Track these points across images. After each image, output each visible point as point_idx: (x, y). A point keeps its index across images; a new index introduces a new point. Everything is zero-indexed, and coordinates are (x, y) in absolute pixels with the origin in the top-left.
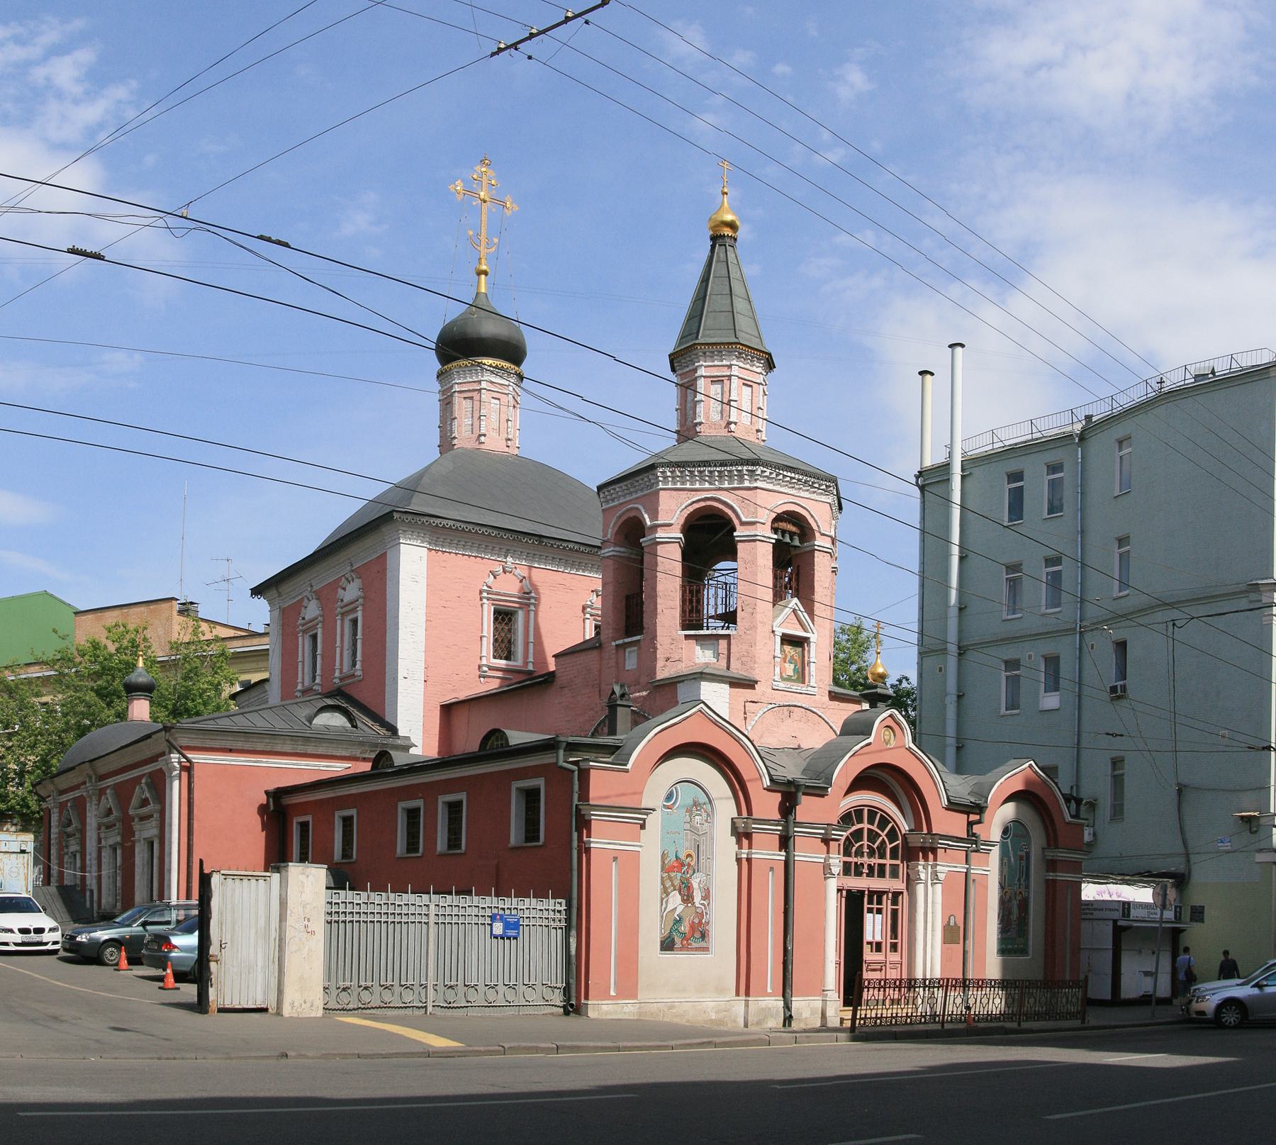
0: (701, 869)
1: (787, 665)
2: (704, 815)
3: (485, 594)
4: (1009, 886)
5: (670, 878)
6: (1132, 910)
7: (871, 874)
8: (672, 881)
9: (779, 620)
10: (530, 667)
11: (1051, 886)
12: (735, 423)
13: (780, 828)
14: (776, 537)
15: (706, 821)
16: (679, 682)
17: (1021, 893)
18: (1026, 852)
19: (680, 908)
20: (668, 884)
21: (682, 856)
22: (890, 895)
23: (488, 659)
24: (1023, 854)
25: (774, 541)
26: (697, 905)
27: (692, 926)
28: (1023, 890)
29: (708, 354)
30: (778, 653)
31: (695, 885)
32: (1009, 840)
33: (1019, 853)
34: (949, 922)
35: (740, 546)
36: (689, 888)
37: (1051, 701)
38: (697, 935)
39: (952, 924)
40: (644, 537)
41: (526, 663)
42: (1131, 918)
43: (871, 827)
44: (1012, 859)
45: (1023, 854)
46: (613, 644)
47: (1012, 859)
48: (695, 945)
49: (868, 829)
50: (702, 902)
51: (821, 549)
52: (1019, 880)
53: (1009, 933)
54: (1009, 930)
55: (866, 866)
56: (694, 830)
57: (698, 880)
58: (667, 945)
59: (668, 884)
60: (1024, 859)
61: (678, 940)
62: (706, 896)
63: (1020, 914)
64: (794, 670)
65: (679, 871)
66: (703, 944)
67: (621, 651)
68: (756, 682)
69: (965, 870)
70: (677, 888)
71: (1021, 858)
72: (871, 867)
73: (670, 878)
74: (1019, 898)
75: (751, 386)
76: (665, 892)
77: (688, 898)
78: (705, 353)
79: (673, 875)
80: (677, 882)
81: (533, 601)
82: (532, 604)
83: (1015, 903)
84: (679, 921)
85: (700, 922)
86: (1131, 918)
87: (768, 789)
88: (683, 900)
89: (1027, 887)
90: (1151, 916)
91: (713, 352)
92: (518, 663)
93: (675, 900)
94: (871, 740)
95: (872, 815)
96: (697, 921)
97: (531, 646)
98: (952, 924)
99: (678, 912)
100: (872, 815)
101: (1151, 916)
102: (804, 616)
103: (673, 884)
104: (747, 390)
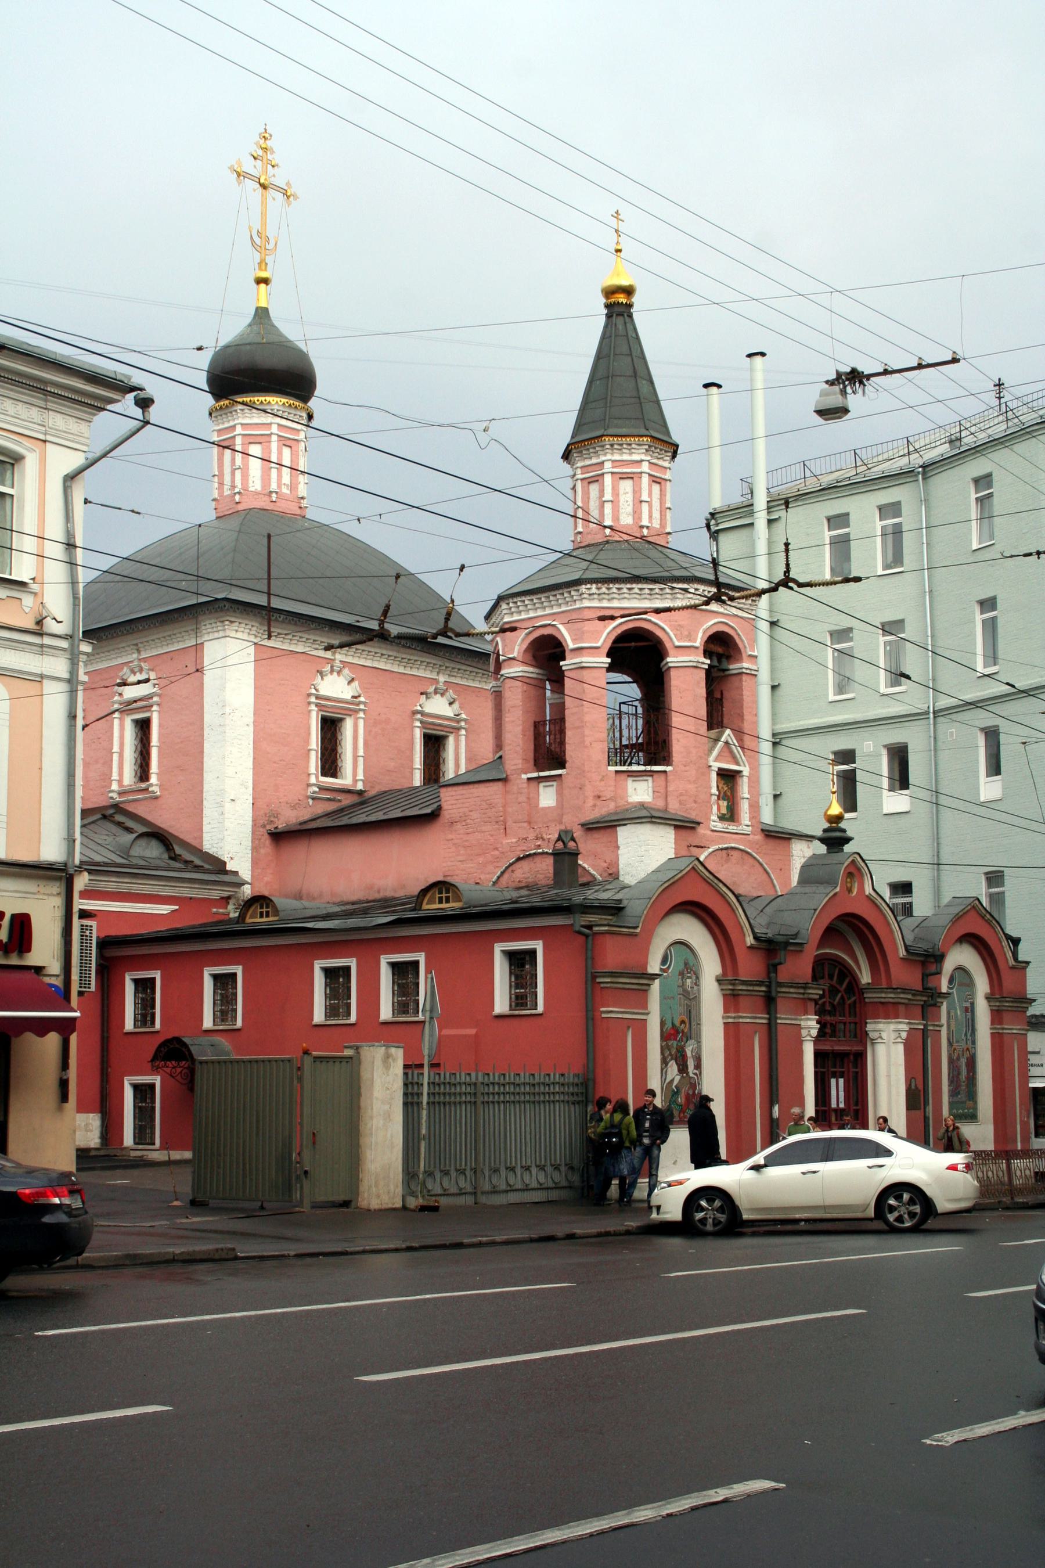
0: (693, 1036)
1: (721, 802)
2: (694, 977)
3: (313, 699)
8: (669, 1050)
9: (715, 753)
10: (360, 786)
13: (763, 989)
14: (708, 661)
15: (696, 984)
16: (620, 825)
17: (968, 1049)
19: (677, 1079)
20: (667, 1053)
21: (677, 1024)
22: (852, 1057)
23: (317, 778)
24: (968, 1005)
25: (707, 667)
26: (691, 1075)
27: (688, 1097)
29: (616, 446)
30: (714, 791)
31: (689, 1054)
35: (673, 673)
36: (684, 1057)
37: (896, 802)
39: (913, 1087)
40: (564, 659)
41: (355, 781)
45: (968, 1005)
46: (524, 776)
50: (695, 1071)
51: (748, 671)
52: (966, 1035)
54: (959, 1093)
56: (686, 994)
59: (667, 1053)
61: (676, 1113)
62: (698, 1066)
64: (728, 807)
65: (675, 1039)
67: (533, 784)
68: (699, 823)
69: (922, 1027)
70: (674, 1056)
71: (966, 1010)
73: (668, 1048)
74: (967, 1054)
75: (659, 483)
76: (664, 1062)
77: (683, 1069)
78: (612, 445)
79: (670, 1043)
80: (674, 1051)
81: (362, 707)
82: (360, 710)
83: (963, 1061)
84: (676, 1093)
85: (694, 1092)
87: (751, 947)
88: (679, 1070)
91: (621, 445)
92: (345, 780)
93: (673, 1069)
94: (838, 889)
96: (691, 1092)
97: (361, 761)
98: (913, 1087)
99: (675, 1083)
102: (737, 750)
103: (670, 1054)
104: (656, 488)
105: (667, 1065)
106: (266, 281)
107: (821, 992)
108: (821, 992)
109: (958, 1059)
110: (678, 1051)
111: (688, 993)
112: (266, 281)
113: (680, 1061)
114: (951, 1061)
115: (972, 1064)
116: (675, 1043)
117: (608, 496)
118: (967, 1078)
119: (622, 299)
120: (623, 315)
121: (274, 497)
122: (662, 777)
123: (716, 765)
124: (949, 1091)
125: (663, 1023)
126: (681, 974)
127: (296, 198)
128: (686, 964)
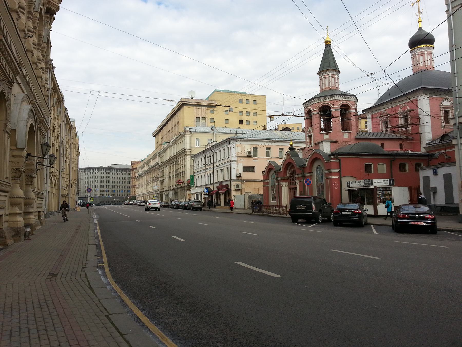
4: (319, 182)
6: (351, 184)
12: (324, 88)
17: (322, 183)
28: (322, 183)
33: (321, 173)
39: (301, 193)
42: (351, 187)
45: (322, 173)
52: (321, 180)
54: (319, 194)
63: (322, 189)
71: (321, 174)
74: (321, 185)
76: (272, 192)
77: (274, 193)
83: (321, 186)
86: (351, 187)
89: (323, 182)
90: (358, 185)
98: (301, 193)
101: (358, 185)
106: (421, 21)
109: (319, 186)
112: (421, 21)
114: (317, 187)
117: (330, 81)
118: (322, 190)
121: (427, 66)
124: (317, 193)
127: (412, 7)
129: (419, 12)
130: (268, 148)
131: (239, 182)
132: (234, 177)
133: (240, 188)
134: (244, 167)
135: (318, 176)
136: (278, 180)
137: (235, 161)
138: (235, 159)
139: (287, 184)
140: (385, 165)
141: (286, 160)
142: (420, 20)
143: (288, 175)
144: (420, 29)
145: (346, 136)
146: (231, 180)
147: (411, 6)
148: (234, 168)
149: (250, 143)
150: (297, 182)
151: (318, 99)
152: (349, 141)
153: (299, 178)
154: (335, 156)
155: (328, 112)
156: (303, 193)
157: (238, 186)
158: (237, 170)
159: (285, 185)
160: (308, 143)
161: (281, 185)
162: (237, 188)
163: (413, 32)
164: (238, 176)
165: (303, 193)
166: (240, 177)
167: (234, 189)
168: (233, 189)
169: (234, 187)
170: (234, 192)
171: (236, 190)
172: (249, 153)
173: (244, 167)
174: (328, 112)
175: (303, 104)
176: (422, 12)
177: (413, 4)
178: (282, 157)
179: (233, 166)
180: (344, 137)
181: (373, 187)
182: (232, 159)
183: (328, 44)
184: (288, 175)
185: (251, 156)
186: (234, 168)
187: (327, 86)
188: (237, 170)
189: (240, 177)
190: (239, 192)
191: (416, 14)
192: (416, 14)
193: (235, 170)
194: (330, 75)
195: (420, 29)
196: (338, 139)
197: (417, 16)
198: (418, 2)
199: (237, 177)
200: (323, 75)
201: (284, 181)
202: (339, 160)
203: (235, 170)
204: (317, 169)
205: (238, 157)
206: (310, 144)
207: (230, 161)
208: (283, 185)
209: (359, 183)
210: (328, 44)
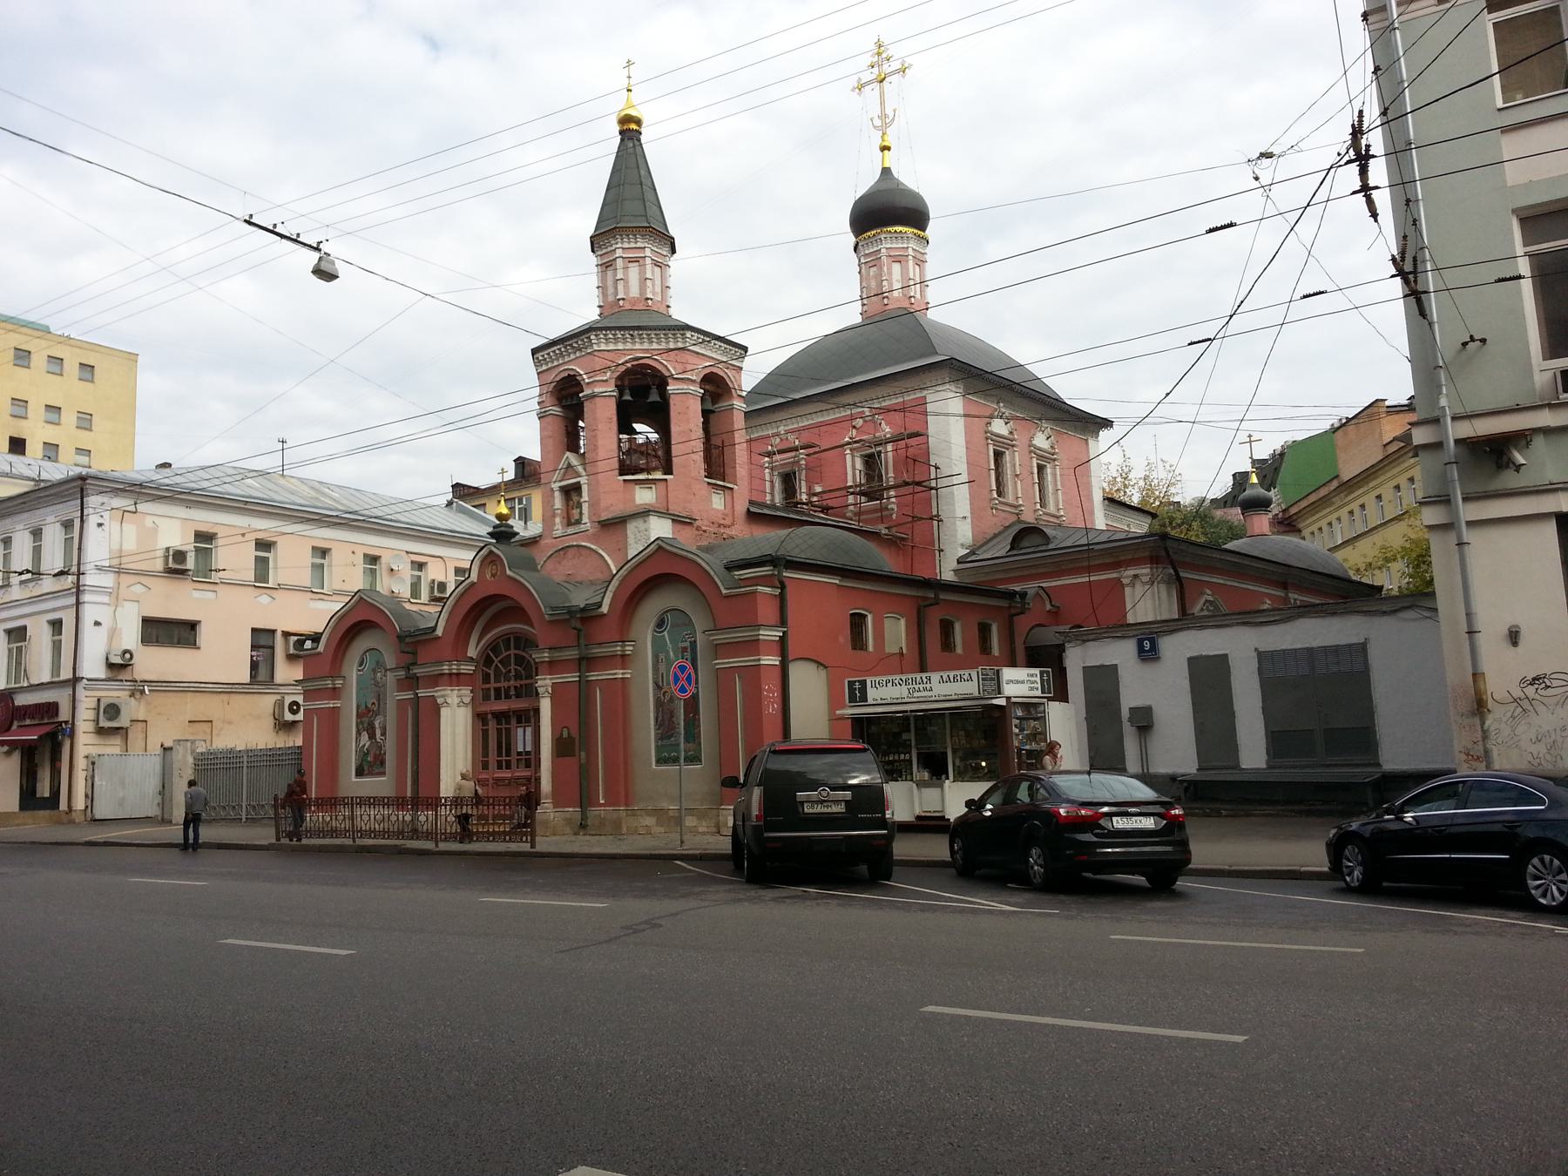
5: (362, 723)
7: (498, 697)
11: (722, 679)
18: (690, 642)
21: (369, 706)
24: (687, 644)
27: (376, 757)
31: (377, 726)
32: (665, 633)
34: (562, 734)
36: (373, 728)
38: (378, 763)
39: (565, 734)
42: (870, 701)
43: (517, 652)
44: (671, 653)
45: (687, 644)
47: (671, 653)
48: (376, 771)
49: (515, 655)
53: (673, 739)
55: (512, 689)
56: (376, 684)
57: (378, 721)
58: (360, 772)
60: (689, 650)
61: (366, 768)
66: (381, 770)
72: (497, 690)
76: (359, 733)
77: (372, 736)
79: (363, 719)
84: (366, 754)
85: (380, 753)
90: (916, 694)
93: (365, 737)
95: (517, 639)
96: (378, 752)
100: (517, 639)
101: (916, 694)
105: (360, 734)
107: (781, 634)
108: (781, 634)
110: (369, 724)
111: (378, 683)
112: (888, 148)
113: (370, 732)
114: (659, 704)
115: (692, 705)
116: (367, 719)
119: (633, 126)
120: (632, 139)
122: (664, 483)
123: (556, 486)
124: (656, 734)
125: (358, 707)
126: (374, 670)
128: (378, 663)
129: (883, 116)
130: (264, 545)
131: (115, 693)
132: (93, 666)
133: (123, 721)
134: (147, 622)
135: (662, 656)
136: (417, 678)
137: (98, 590)
138: (108, 580)
139: (466, 692)
140: (903, 622)
141: (473, 584)
142: (886, 144)
143: (472, 652)
144: (886, 171)
145: (718, 502)
146: (75, 680)
147: (853, 90)
148: (97, 624)
149: (180, 512)
150: (544, 683)
151: (605, 335)
152: (727, 522)
153: (553, 666)
154: (765, 570)
155: (654, 397)
156: (575, 734)
157: (113, 710)
158: (113, 633)
159: (456, 700)
160: (558, 520)
161: (440, 701)
162: (110, 719)
163: (864, 181)
164: (118, 660)
165: (575, 734)
166: (123, 667)
167: (90, 727)
168: (84, 725)
169: (91, 715)
170: (92, 739)
171: (101, 731)
172: (180, 556)
173: (147, 622)
174: (654, 397)
175: (534, 351)
176: (893, 119)
177: (860, 87)
178: (323, 588)
179: (89, 613)
180: (714, 506)
181: (1002, 702)
182: (89, 580)
183: (630, 130)
184: (472, 652)
185: (183, 572)
186: (97, 624)
187: (634, 291)
188: (113, 633)
189: (123, 667)
190: (117, 740)
191: (872, 120)
192: (872, 120)
193: (102, 632)
194: (648, 252)
195: (886, 171)
196: (694, 509)
197: (875, 127)
198: (881, 81)
199: (111, 666)
200: (619, 245)
201: (456, 679)
202: (783, 587)
203: (102, 632)
204: (660, 624)
205: (119, 571)
206: (565, 521)
207: (78, 590)
208: (449, 701)
209: (921, 686)
210: (630, 130)
